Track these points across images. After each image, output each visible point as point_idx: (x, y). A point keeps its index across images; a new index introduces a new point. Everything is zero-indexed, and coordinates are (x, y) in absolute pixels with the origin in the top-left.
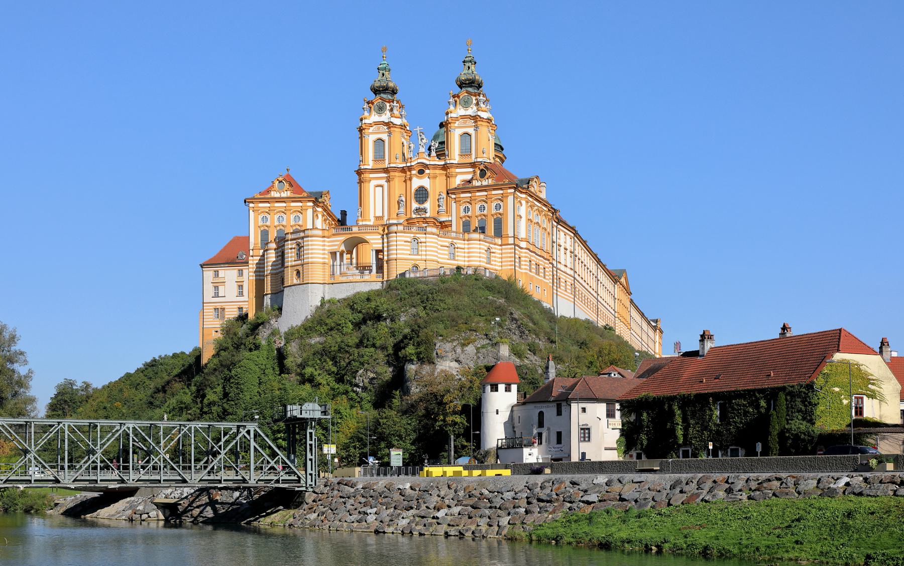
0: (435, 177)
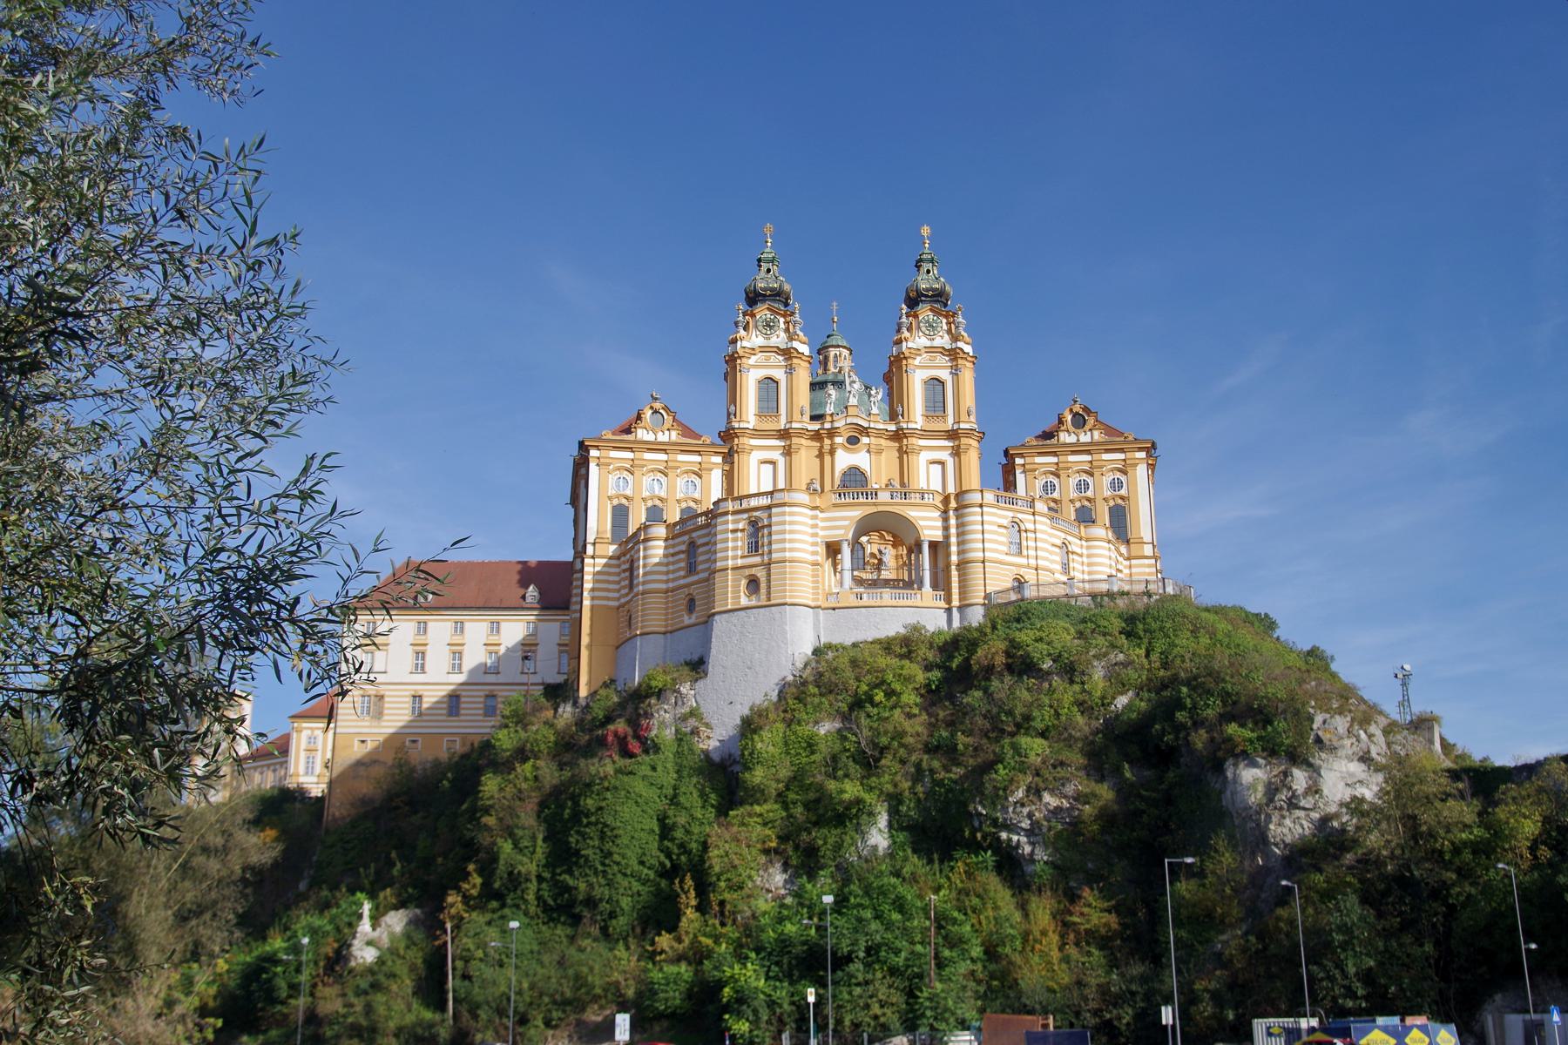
0: (879, 452)
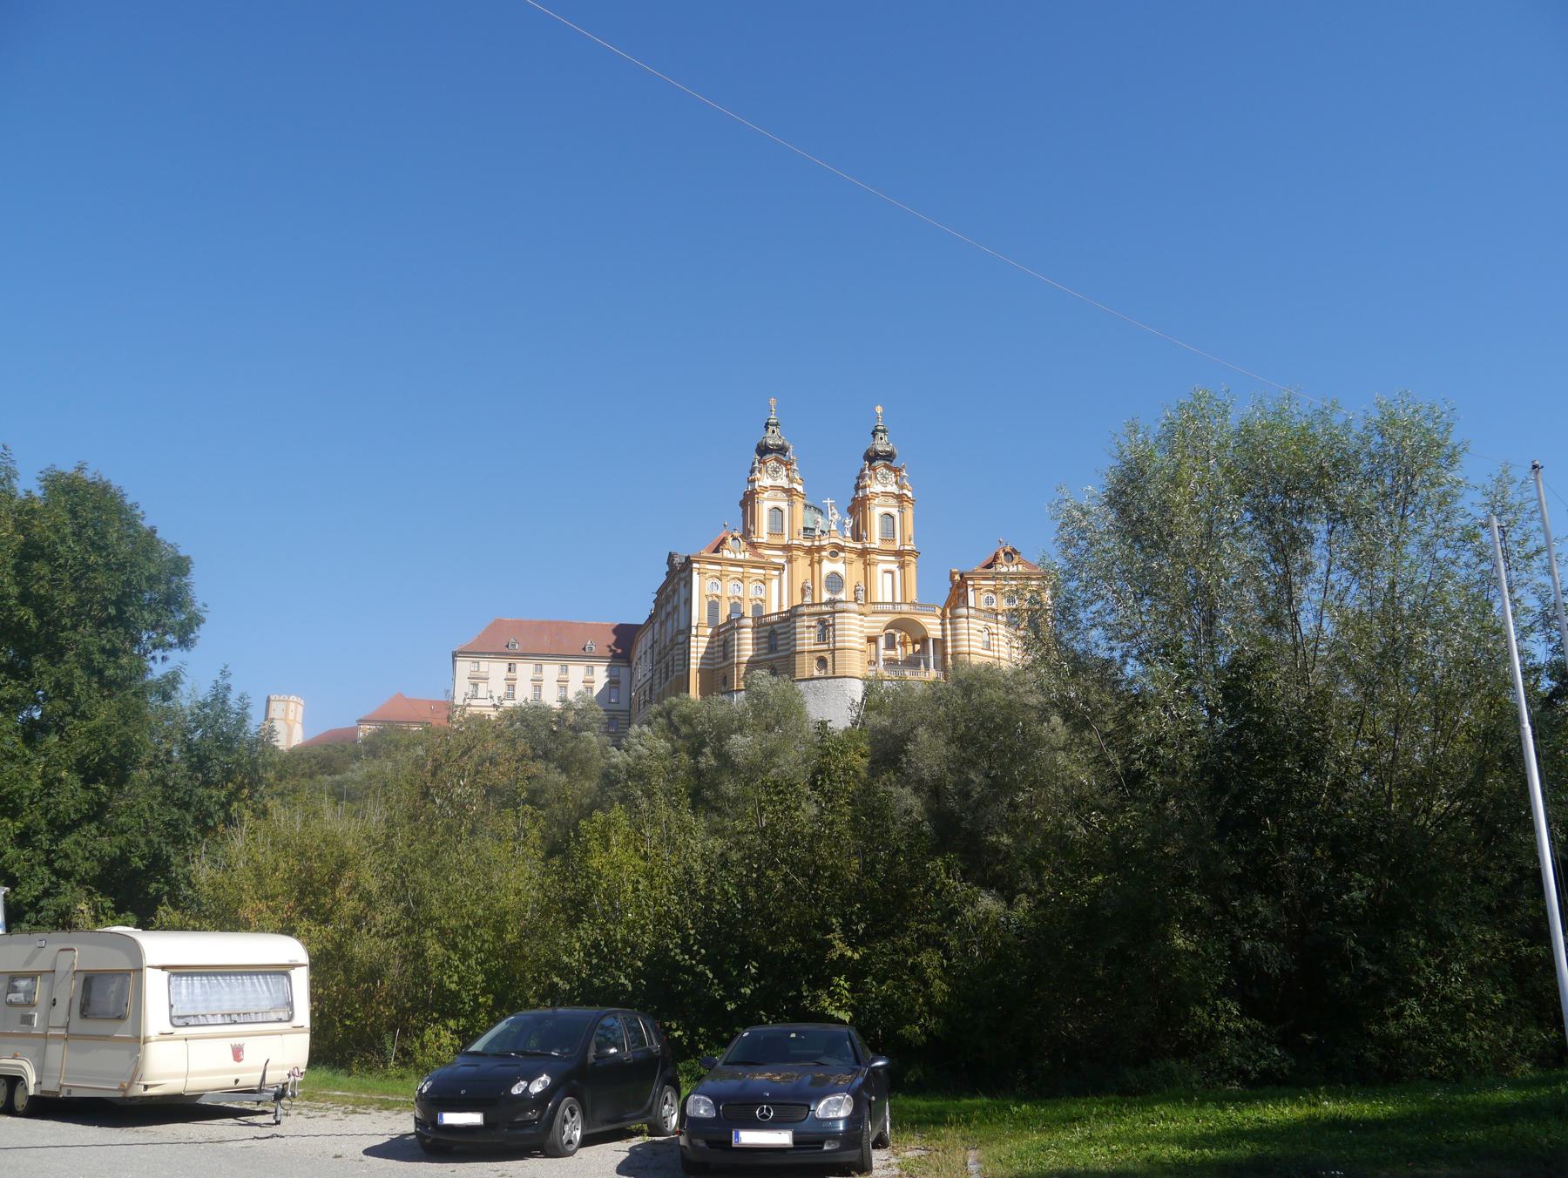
0: (851, 563)
